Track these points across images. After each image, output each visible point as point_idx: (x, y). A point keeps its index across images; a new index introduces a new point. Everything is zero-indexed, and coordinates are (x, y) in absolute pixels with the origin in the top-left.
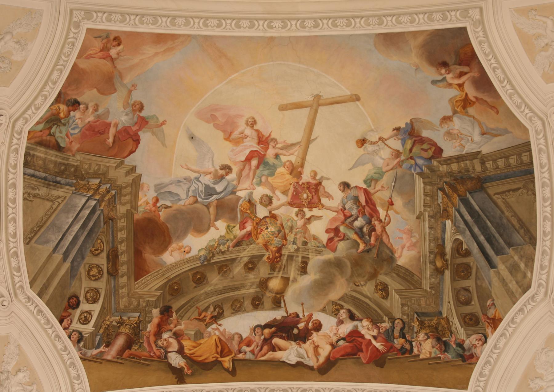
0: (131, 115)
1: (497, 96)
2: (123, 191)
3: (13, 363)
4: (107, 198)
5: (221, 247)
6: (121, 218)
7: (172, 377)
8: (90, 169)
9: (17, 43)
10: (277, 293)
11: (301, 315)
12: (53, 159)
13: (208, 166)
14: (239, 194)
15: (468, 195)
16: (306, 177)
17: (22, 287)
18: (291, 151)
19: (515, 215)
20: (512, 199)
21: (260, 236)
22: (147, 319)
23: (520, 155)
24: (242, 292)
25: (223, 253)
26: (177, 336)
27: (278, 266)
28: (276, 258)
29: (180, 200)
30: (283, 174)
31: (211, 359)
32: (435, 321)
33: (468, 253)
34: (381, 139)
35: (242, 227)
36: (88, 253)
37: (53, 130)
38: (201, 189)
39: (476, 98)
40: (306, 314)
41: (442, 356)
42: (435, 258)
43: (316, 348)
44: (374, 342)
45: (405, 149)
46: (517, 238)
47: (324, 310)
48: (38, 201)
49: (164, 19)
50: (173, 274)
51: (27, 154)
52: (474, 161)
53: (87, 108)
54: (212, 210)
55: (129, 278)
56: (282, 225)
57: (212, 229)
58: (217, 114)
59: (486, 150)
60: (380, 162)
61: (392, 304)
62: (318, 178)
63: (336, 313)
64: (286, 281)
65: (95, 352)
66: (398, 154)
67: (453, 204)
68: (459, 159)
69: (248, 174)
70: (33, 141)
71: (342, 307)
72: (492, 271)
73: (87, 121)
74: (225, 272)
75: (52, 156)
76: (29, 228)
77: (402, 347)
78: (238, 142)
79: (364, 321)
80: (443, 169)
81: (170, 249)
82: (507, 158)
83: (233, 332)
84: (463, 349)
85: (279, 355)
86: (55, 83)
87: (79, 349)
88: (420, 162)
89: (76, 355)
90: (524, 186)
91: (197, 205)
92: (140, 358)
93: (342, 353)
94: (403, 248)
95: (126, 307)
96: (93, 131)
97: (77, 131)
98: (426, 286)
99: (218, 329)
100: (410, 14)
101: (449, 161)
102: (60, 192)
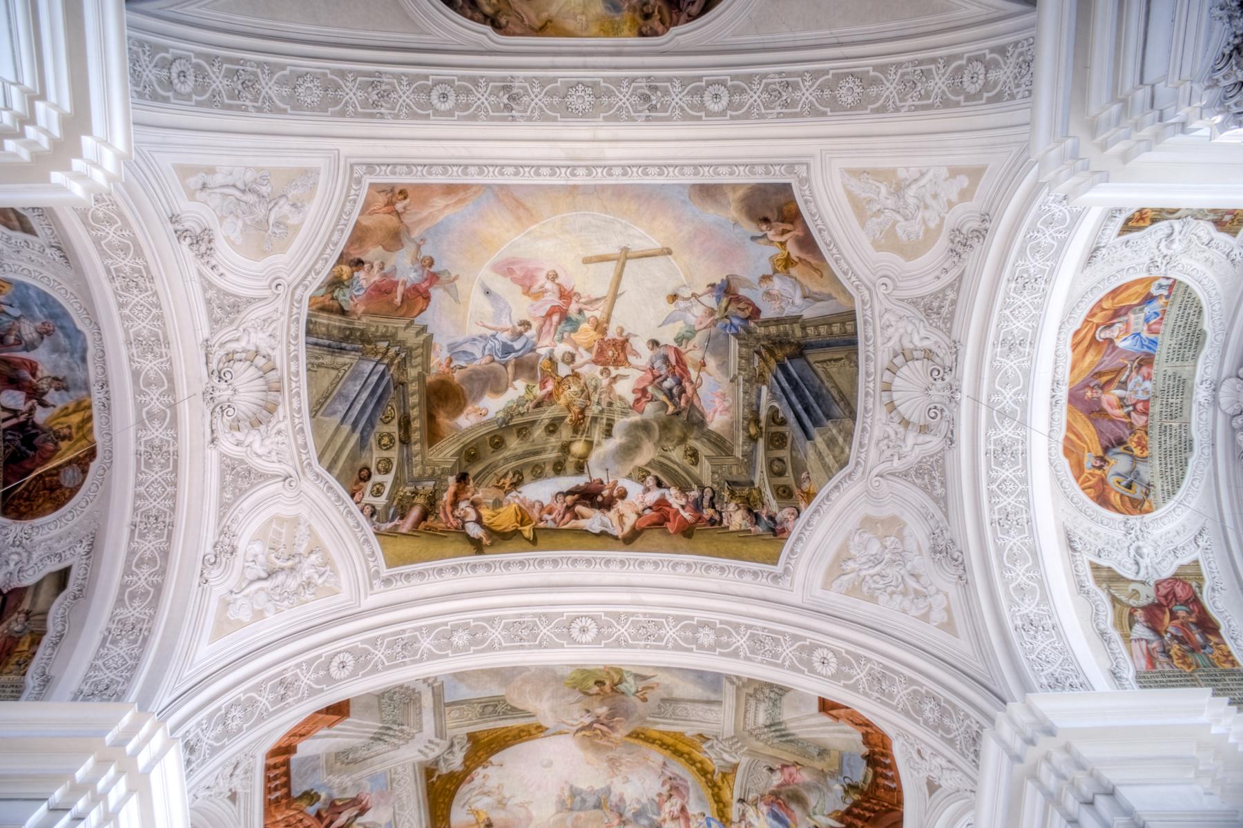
0: (420, 272)
1: (822, 259)
2: (413, 353)
3: (305, 545)
4: (396, 361)
5: (520, 408)
6: (412, 382)
7: (470, 547)
8: (377, 331)
9: (293, 205)
10: (580, 458)
11: (605, 482)
12: (337, 324)
13: (506, 323)
14: (539, 351)
15: (786, 361)
16: (612, 333)
17: (310, 464)
18: (596, 306)
19: (836, 386)
20: (833, 369)
21: (562, 396)
22: (443, 488)
23: (843, 323)
24: (543, 456)
25: (522, 415)
26: (475, 504)
27: (581, 428)
28: (579, 420)
29: (475, 359)
30: (586, 331)
31: (512, 529)
32: (746, 491)
33: (784, 422)
34: (693, 295)
35: (543, 385)
36: (379, 422)
37: (335, 294)
38: (498, 346)
39: (800, 259)
40: (611, 481)
41: (752, 529)
42: (749, 424)
43: (621, 516)
44: (682, 512)
45: (720, 307)
46: (837, 410)
47: (629, 477)
48: (323, 370)
49: (455, 169)
50: (468, 439)
51: (309, 322)
52: (795, 325)
53: (372, 267)
54: (510, 369)
55: (422, 445)
56: (585, 384)
57: (510, 390)
58: (514, 267)
59: (808, 314)
60: (692, 320)
61: (701, 472)
62: (624, 334)
63: (642, 480)
64: (590, 444)
65: (389, 525)
66: (712, 312)
67: (770, 369)
68: (778, 321)
69: (549, 331)
70: (314, 307)
71: (649, 474)
72: (808, 443)
73: (372, 281)
74: (525, 436)
75: (336, 321)
76: (314, 400)
77: (711, 518)
78: (538, 296)
79: (672, 488)
80: (761, 331)
81: (466, 411)
82: (830, 325)
83: (533, 500)
84: (775, 522)
85: (582, 523)
86: (336, 245)
87: (373, 524)
88: (736, 322)
89: (369, 530)
90: (847, 357)
91: (495, 365)
92: (436, 529)
93: (649, 522)
94: (715, 412)
95: (420, 476)
96: (380, 291)
97: (361, 292)
98: (738, 453)
99: (517, 497)
100: (730, 165)
101: (767, 323)
102: (346, 359)
